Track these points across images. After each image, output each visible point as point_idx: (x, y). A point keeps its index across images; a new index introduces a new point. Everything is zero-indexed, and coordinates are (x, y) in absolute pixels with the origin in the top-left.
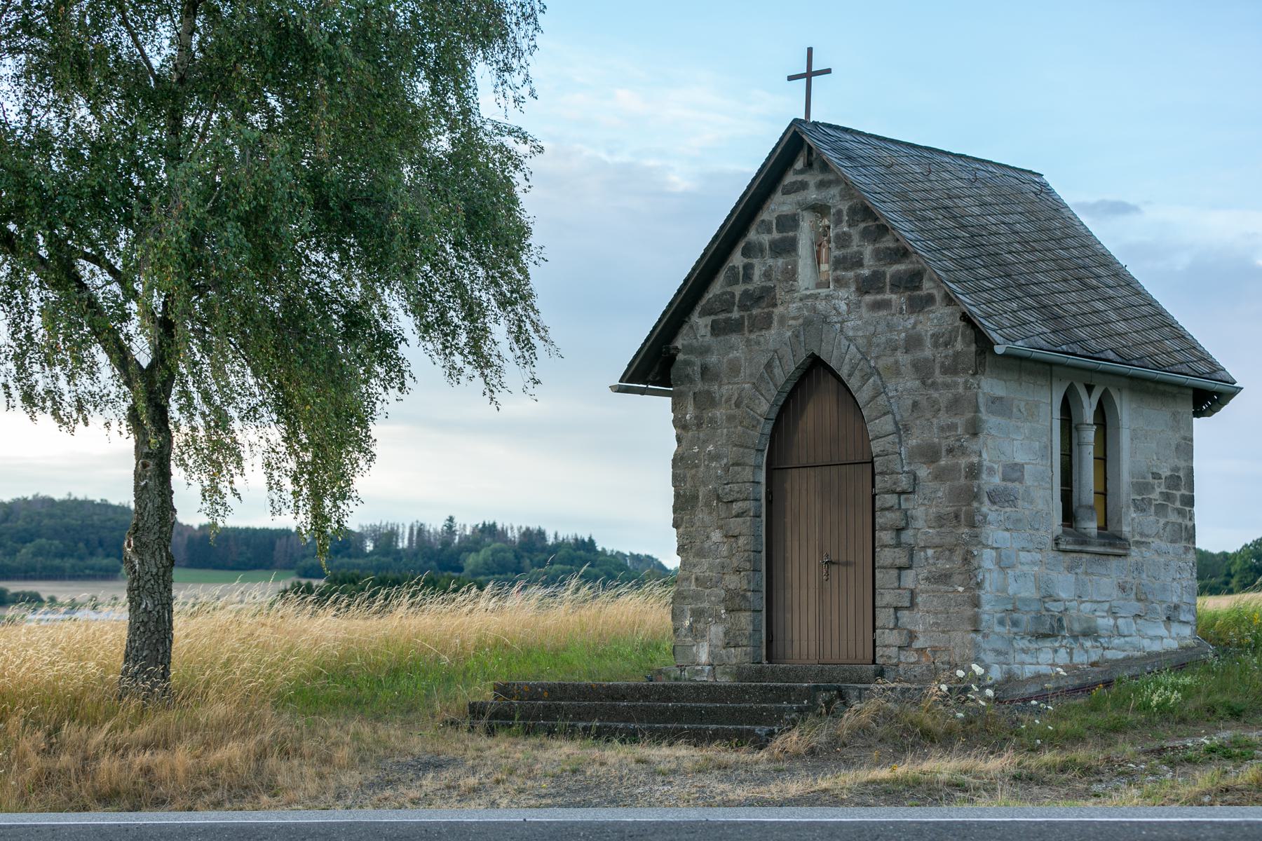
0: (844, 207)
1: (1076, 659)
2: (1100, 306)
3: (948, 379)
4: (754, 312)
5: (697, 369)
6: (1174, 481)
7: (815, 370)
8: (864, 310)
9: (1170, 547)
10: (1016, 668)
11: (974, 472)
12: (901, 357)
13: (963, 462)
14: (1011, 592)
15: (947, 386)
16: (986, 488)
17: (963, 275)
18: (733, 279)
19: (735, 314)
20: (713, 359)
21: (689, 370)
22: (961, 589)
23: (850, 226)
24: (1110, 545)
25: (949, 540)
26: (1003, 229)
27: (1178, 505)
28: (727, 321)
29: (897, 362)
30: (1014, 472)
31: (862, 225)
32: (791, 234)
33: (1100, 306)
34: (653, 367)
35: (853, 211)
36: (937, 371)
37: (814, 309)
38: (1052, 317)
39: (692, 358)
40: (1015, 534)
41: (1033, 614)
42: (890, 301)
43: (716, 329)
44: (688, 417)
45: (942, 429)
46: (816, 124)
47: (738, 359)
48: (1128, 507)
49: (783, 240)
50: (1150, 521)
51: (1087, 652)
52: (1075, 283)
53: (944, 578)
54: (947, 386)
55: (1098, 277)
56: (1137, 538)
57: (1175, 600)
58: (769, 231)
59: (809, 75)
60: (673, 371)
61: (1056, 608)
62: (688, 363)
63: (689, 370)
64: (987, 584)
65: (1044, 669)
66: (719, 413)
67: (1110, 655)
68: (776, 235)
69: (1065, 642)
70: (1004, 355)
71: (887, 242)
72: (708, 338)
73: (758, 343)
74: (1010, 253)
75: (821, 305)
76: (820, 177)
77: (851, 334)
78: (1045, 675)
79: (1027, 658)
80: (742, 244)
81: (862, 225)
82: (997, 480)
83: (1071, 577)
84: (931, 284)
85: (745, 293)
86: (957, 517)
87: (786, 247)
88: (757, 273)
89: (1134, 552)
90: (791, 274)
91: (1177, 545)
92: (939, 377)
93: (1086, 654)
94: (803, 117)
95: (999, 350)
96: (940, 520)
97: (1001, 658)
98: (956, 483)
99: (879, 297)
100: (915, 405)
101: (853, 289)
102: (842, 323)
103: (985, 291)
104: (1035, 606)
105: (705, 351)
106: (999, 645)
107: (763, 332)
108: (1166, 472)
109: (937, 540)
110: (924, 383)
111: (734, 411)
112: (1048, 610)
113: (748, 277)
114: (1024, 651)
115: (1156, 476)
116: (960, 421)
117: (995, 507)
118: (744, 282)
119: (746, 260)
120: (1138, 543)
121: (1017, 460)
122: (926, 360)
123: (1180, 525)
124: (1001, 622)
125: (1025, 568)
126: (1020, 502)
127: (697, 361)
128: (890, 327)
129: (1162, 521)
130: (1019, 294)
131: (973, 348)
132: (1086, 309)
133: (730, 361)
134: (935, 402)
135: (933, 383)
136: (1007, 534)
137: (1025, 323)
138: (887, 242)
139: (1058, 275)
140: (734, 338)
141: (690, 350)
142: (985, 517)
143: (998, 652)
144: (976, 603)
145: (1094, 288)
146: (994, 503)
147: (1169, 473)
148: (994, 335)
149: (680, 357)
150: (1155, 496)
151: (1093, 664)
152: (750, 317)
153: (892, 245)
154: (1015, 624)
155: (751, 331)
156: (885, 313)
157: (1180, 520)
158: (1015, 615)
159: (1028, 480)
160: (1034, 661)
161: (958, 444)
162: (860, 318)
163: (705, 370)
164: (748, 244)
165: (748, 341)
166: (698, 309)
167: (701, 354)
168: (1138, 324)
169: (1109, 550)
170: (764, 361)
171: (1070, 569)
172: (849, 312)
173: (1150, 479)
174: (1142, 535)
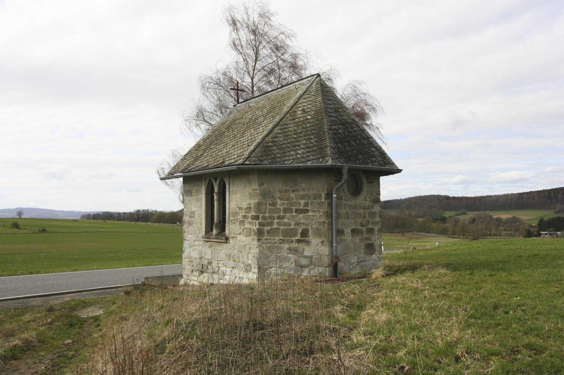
27: (250, 220)
56: (232, 235)
89: (231, 241)
91: (249, 238)
115: (240, 209)
123: (250, 229)
129: (242, 227)
147: (246, 206)
150: (240, 217)
157: (251, 227)
169: (219, 241)
173: (238, 210)
174: (234, 234)
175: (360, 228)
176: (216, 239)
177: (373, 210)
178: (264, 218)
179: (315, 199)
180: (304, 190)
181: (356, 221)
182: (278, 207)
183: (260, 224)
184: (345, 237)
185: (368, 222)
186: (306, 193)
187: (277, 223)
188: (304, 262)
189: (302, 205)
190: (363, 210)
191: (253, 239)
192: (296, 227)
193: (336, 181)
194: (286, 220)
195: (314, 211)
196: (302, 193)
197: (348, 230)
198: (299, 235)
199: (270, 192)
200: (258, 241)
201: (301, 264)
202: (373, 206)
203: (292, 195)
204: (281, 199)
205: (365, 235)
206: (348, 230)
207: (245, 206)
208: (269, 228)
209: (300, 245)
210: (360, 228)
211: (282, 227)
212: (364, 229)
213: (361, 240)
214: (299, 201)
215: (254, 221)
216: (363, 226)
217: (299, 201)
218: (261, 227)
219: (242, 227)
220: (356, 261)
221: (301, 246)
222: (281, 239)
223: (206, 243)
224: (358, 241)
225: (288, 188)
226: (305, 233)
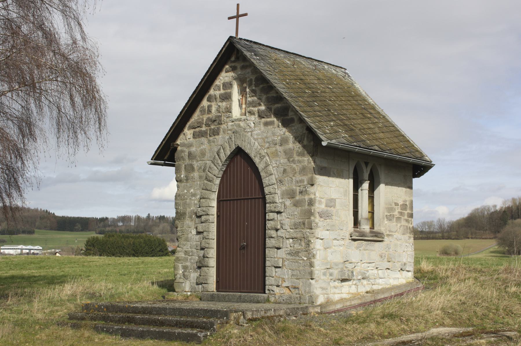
0: (253, 78)
1: (360, 290)
2: (371, 126)
3: (300, 158)
4: (212, 127)
5: (187, 154)
6: (404, 207)
7: (239, 153)
8: (262, 125)
9: (402, 237)
10: (331, 296)
11: (311, 203)
12: (278, 148)
13: (307, 198)
14: (329, 259)
15: (299, 162)
16: (317, 210)
17: (308, 109)
18: (203, 112)
19: (204, 128)
20: (193, 149)
21: (183, 154)
22: (305, 259)
23: (255, 86)
24: (376, 236)
25: (299, 235)
26: (327, 90)
27: (406, 217)
28: (200, 132)
29: (276, 150)
30: (331, 203)
31: (261, 86)
32: (229, 91)
33: (371, 126)
34: (166, 153)
35: (257, 79)
36: (295, 155)
37: (239, 126)
38: (349, 130)
39: (184, 149)
40: (331, 232)
41: (339, 270)
42: (274, 121)
43: (195, 136)
44: (182, 176)
45: (297, 182)
46: (241, 39)
47: (205, 149)
48: (384, 219)
49: (226, 93)
50: (394, 225)
51: (364, 286)
52: (361, 116)
53: (296, 253)
54: (299, 162)
55: (371, 113)
56: (388, 233)
57: (404, 261)
58: (219, 90)
59: (238, 16)
60: (176, 155)
61: (350, 266)
62: (182, 151)
63: (183, 154)
64: (318, 257)
65: (345, 296)
66: (196, 174)
67: (375, 287)
68: (222, 91)
69: (354, 282)
70: (328, 147)
71: (272, 94)
72: (192, 139)
73: (214, 142)
74: (330, 100)
75: (242, 124)
76: (242, 64)
77: (255, 137)
78: (345, 299)
79: (337, 291)
80: (207, 96)
81: (261, 86)
82: (323, 206)
83: (358, 251)
84: (293, 113)
85: (208, 119)
86: (304, 224)
87: (227, 97)
88: (214, 109)
89: (386, 239)
90: (229, 110)
91: (405, 236)
92: (297, 158)
93: (364, 287)
94: (234, 35)
95: (324, 144)
96: (295, 226)
97: (324, 291)
98: (303, 208)
99: (269, 120)
100: (285, 171)
101: (257, 116)
102: (251, 132)
103: (318, 116)
104: (341, 266)
105: (190, 145)
106: (324, 285)
107: (216, 137)
108: (401, 202)
109: (295, 235)
110: (289, 160)
111: (203, 174)
112: (346, 267)
113: (209, 111)
114: (335, 287)
115: (396, 204)
116: (305, 178)
117: (322, 219)
118: (208, 113)
119: (209, 103)
120: (388, 235)
121: (333, 197)
122: (290, 149)
123: (407, 227)
124: (324, 274)
125: (336, 248)
126: (334, 217)
127: (187, 150)
128: (274, 134)
129: (399, 225)
130: (334, 119)
131: (312, 143)
132: (365, 127)
133: (202, 150)
134: (294, 169)
135: (293, 161)
136: (328, 232)
137: (336, 132)
138: (272, 94)
139: (353, 112)
140: (203, 140)
141: (183, 145)
142: (317, 224)
143: (323, 289)
144: (311, 265)
145: (369, 118)
146: (321, 217)
147: (402, 203)
148: (321, 137)
149: (179, 148)
150: (396, 213)
151: (367, 292)
152: (210, 130)
153: (275, 95)
154: (331, 275)
155: (210, 136)
156: (271, 127)
157: (407, 224)
158: (331, 270)
159: (338, 206)
160: (340, 292)
161: (304, 189)
162: (260, 130)
163: (190, 154)
164: (210, 95)
165: (209, 141)
166: (187, 126)
167: (188, 147)
168: (388, 135)
170: (216, 150)
171: (357, 248)
172: (255, 127)
174: (390, 231)
191: (410, 237)
219: (399, 225)
223: (353, 242)
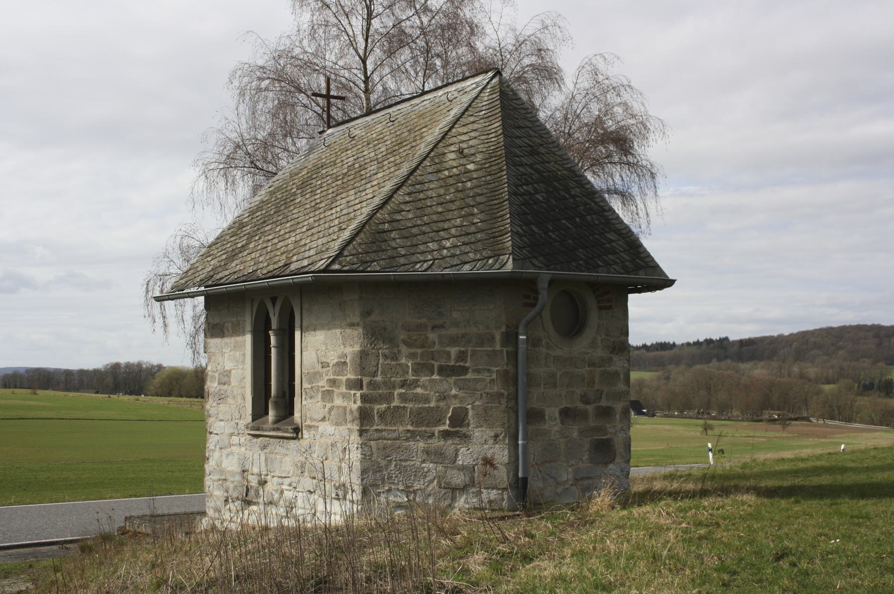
27: (343, 389)
56: (308, 423)
89: (306, 434)
91: (341, 428)
115: (325, 365)
121: (226, 368)
123: (345, 408)
129: (329, 405)
147: (336, 361)
150: (323, 383)
157: (345, 404)
169: (280, 434)
173: (318, 368)
174: (312, 419)
175: (580, 406)
176: (274, 430)
177: (613, 368)
178: (373, 385)
179: (482, 344)
180: (456, 325)
181: (573, 392)
182: (403, 361)
183: (364, 398)
184: (546, 427)
185: (599, 395)
186: (463, 331)
187: (401, 395)
188: (458, 479)
189: (453, 357)
190: (587, 368)
192: (442, 404)
193: (526, 305)
194: (419, 390)
195: (478, 371)
196: (453, 331)
197: (552, 412)
198: (448, 422)
199: (385, 329)
200: (361, 435)
201: (448, 483)
202: (610, 360)
203: (432, 336)
204: (408, 345)
205: (592, 422)
206: (552, 412)
207: (333, 359)
208: (384, 406)
209: (450, 442)
210: (580, 406)
211: (410, 405)
212: (590, 408)
213: (581, 433)
214: (448, 349)
215: (353, 392)
216: (587, 402)
217: (448, 349)
218: (367, 405)
219: (329, 405)
220: (570, 477)
221: (449, 446)
222: (408, 431)
223: (255, 440)
224: (575, 434)
225: (424, 320)
226: (459, 419)
